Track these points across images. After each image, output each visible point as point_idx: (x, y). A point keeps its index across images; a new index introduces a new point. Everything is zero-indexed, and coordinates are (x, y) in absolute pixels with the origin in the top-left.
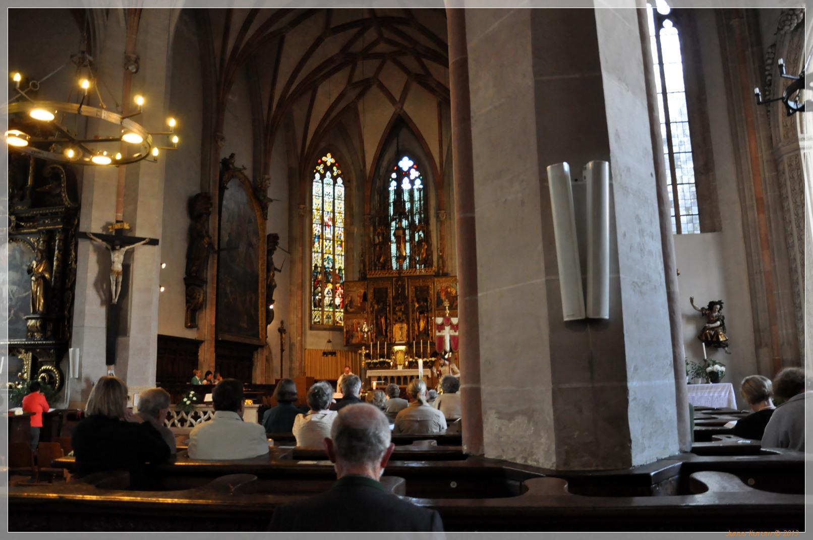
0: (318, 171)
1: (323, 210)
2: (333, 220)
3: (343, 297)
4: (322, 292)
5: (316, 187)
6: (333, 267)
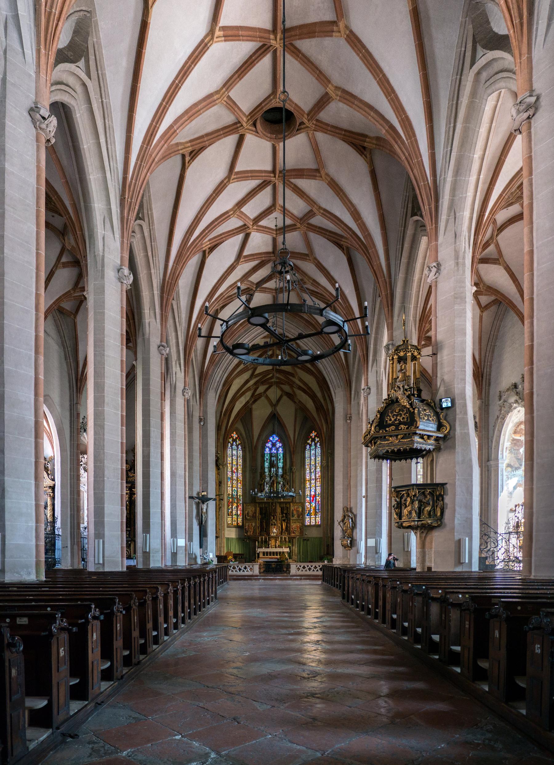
0: (229, 442)
2: (237, 469)
3: (243, 510)
4: (232, 508)
5: (229, 452)
6: (237, 495)
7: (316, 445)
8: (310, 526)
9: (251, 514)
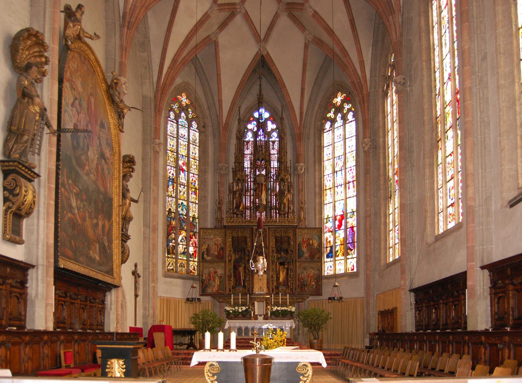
1: (177, 152)
2: (188, 164)
3: (198, 246)
4: (176, 239)
5: (171, 128)
6: (187, 214)
7: (344, 118)
8: (335, 276)
9: (214, 251)
